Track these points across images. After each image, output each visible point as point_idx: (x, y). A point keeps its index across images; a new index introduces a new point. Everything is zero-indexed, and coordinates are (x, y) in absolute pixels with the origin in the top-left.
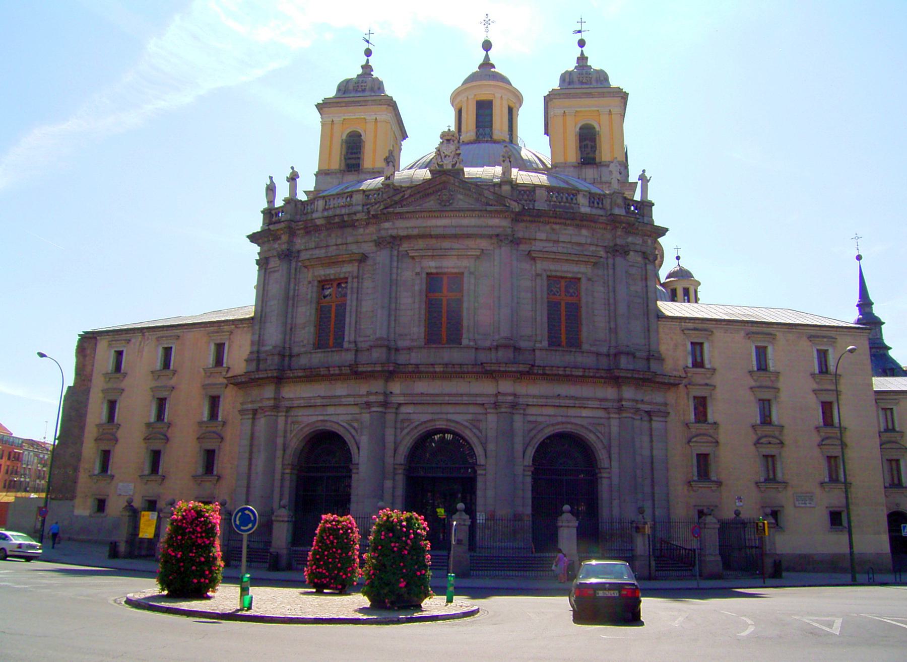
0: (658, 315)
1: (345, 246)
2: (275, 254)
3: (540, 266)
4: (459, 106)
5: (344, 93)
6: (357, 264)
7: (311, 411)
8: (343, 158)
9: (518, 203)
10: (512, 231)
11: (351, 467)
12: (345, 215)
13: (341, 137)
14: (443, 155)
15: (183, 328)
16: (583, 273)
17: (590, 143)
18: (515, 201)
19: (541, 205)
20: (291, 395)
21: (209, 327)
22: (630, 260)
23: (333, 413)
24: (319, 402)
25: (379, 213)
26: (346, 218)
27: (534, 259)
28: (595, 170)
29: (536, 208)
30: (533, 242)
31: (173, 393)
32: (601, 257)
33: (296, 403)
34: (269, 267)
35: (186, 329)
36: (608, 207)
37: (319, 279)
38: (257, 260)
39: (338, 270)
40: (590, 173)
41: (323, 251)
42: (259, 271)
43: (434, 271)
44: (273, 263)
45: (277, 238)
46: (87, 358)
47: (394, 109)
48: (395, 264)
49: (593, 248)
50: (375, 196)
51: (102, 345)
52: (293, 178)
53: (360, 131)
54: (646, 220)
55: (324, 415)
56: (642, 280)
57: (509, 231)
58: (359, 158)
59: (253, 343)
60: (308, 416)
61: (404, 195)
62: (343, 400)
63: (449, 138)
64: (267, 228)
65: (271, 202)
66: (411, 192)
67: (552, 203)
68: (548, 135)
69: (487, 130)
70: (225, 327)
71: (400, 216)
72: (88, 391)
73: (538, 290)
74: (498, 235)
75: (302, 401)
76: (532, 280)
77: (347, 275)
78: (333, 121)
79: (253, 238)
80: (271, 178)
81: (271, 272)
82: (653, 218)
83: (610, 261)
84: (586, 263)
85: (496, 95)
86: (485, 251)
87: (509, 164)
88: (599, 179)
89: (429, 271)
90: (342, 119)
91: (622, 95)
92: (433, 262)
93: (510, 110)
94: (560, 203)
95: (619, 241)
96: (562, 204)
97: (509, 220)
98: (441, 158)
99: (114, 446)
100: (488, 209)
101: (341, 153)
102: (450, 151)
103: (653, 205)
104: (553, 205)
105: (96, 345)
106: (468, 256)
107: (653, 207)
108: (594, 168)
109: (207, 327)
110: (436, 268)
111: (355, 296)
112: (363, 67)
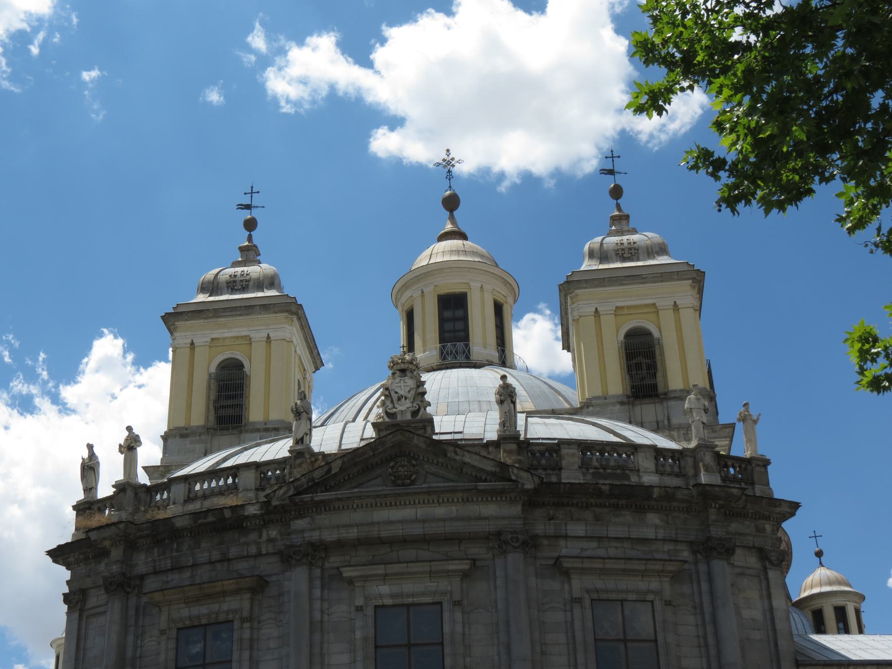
0: (796, 660)
1: (226, 564)
2: (100, 582)
3: (577, 584)
4: (406, 308)
5: (210, 296)
6: (248, 596)
8: (211, 408)
9: (532, 475)
10: (524, 524)
13: (208, 371)
14: (395, 397)
16: (656, 593)
17: (644, 361)
18: (526, 471)
19: (571, 475)
22: (736, 563)
25: (288, 501)
27: (566, 574)
28: (658, 406)
29: (563, 481)
30: (562, 543)
32: (686, 562)
34: (88, 606)
36: (691, 472)
37: (180, 625)
38: (64, 594)
39: (215, 607)
40: (649, 410)
41: (187, 574)
42: (69, 613)
43: (388, 601)
45: (103, 554)
47: (299, 319)
48: (317, 593)
49: (668, 547)
50: (278, 472)
52: (130, 446)
53: (239, 357)
54: (758, 490)
56: (761, 598)
57: (519, 524)
58: (240, 406)
61: (330, 470)
63: (403, 366)
64: (83, 536)
65: (90, 488)
66: (343, 463)
67: (591, 471)
68: (569, 351)
69: (460, 345)
71: (323, 506)
73: (577, 625)
74: (499, 534)
76: (565, 611)
77: (231, 617)
78: (192, 343)
79: (58, 554)
80: (90, 447)
82: (771, 486)
83: (702, 567)
84: (660, 573)
85: (472, 284)
86: (478, 563)
87: (512, 405)
88: (666, 422)
89: (380, 603)
90: (209, 339)
91: (695, 276)
92: (387, 587)
93: (498, 309)
94: (605, 469)
95: (716, 532)
96: (609, 471)
97: (519, 507)
98: (392, 402)
100: (480, 488)
101: (208, 397)
102: (408, 389)
103: (766, 463)
104: (593, 473)
106: (448, 574)
107: (769, 468)
108: (655, 403)
110: (392, 596)
111: (246, 654)
112: (242, 249)
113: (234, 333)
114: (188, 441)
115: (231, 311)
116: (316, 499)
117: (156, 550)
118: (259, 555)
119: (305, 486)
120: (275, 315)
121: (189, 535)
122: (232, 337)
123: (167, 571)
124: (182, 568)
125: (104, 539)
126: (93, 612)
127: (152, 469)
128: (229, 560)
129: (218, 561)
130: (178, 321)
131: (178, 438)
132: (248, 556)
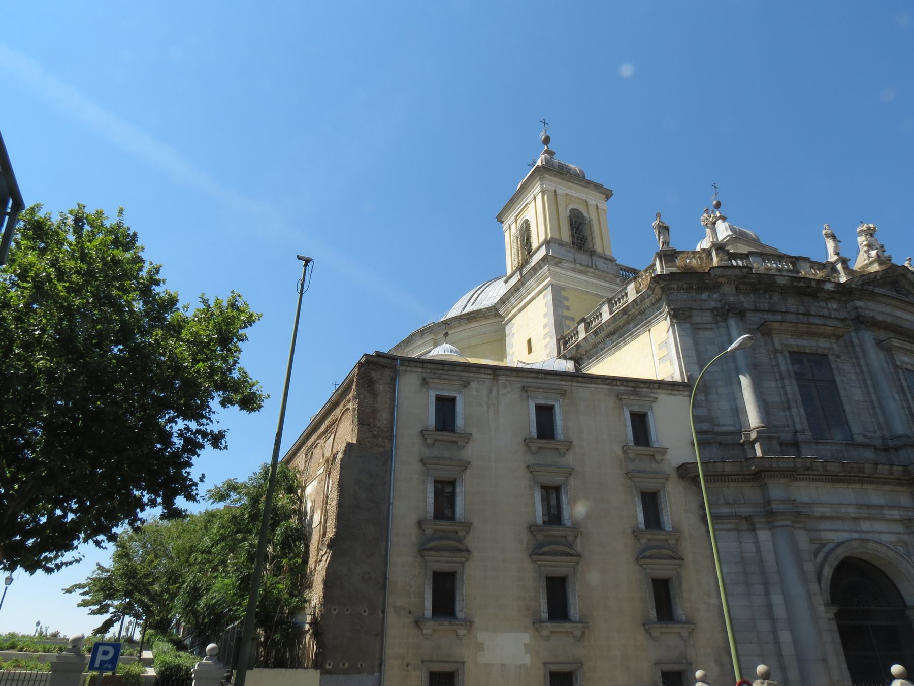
1: (806, 317)
7: (837, 525)
12: (814, 279)
15: (575, 379)
20: (806, 499)
21: (619, 386)
24: (852, 511)
33: (818, 511)
37: (790, 349)
39: (814, 343)
41: (779, 317)
46: (380, 399)
51: (408, 384)
55: (859, 532)
59: (697, 419)
60: (836, 531)
62: (886, 512)
63: (872, 232)
70: (645, 390)
72: (387, 457)
77: (826, 352)
90: (565, 193)
99: (463, 563)
105: (393, 380)
109: (616, 385)
113: (578, 195)
115: (578, 181)
116: (876, 291)
117: (752, 295)
118: (830, 317)
119: (866, 281)
120: (598, 194)
121: (780, 291)
122: (576, 197)
123: (763, 311)
125: (724, 276)
126: (699, 326)
127: (551, 257)
128: (810, 315)
129: (802, 314)
132: (823, 316)
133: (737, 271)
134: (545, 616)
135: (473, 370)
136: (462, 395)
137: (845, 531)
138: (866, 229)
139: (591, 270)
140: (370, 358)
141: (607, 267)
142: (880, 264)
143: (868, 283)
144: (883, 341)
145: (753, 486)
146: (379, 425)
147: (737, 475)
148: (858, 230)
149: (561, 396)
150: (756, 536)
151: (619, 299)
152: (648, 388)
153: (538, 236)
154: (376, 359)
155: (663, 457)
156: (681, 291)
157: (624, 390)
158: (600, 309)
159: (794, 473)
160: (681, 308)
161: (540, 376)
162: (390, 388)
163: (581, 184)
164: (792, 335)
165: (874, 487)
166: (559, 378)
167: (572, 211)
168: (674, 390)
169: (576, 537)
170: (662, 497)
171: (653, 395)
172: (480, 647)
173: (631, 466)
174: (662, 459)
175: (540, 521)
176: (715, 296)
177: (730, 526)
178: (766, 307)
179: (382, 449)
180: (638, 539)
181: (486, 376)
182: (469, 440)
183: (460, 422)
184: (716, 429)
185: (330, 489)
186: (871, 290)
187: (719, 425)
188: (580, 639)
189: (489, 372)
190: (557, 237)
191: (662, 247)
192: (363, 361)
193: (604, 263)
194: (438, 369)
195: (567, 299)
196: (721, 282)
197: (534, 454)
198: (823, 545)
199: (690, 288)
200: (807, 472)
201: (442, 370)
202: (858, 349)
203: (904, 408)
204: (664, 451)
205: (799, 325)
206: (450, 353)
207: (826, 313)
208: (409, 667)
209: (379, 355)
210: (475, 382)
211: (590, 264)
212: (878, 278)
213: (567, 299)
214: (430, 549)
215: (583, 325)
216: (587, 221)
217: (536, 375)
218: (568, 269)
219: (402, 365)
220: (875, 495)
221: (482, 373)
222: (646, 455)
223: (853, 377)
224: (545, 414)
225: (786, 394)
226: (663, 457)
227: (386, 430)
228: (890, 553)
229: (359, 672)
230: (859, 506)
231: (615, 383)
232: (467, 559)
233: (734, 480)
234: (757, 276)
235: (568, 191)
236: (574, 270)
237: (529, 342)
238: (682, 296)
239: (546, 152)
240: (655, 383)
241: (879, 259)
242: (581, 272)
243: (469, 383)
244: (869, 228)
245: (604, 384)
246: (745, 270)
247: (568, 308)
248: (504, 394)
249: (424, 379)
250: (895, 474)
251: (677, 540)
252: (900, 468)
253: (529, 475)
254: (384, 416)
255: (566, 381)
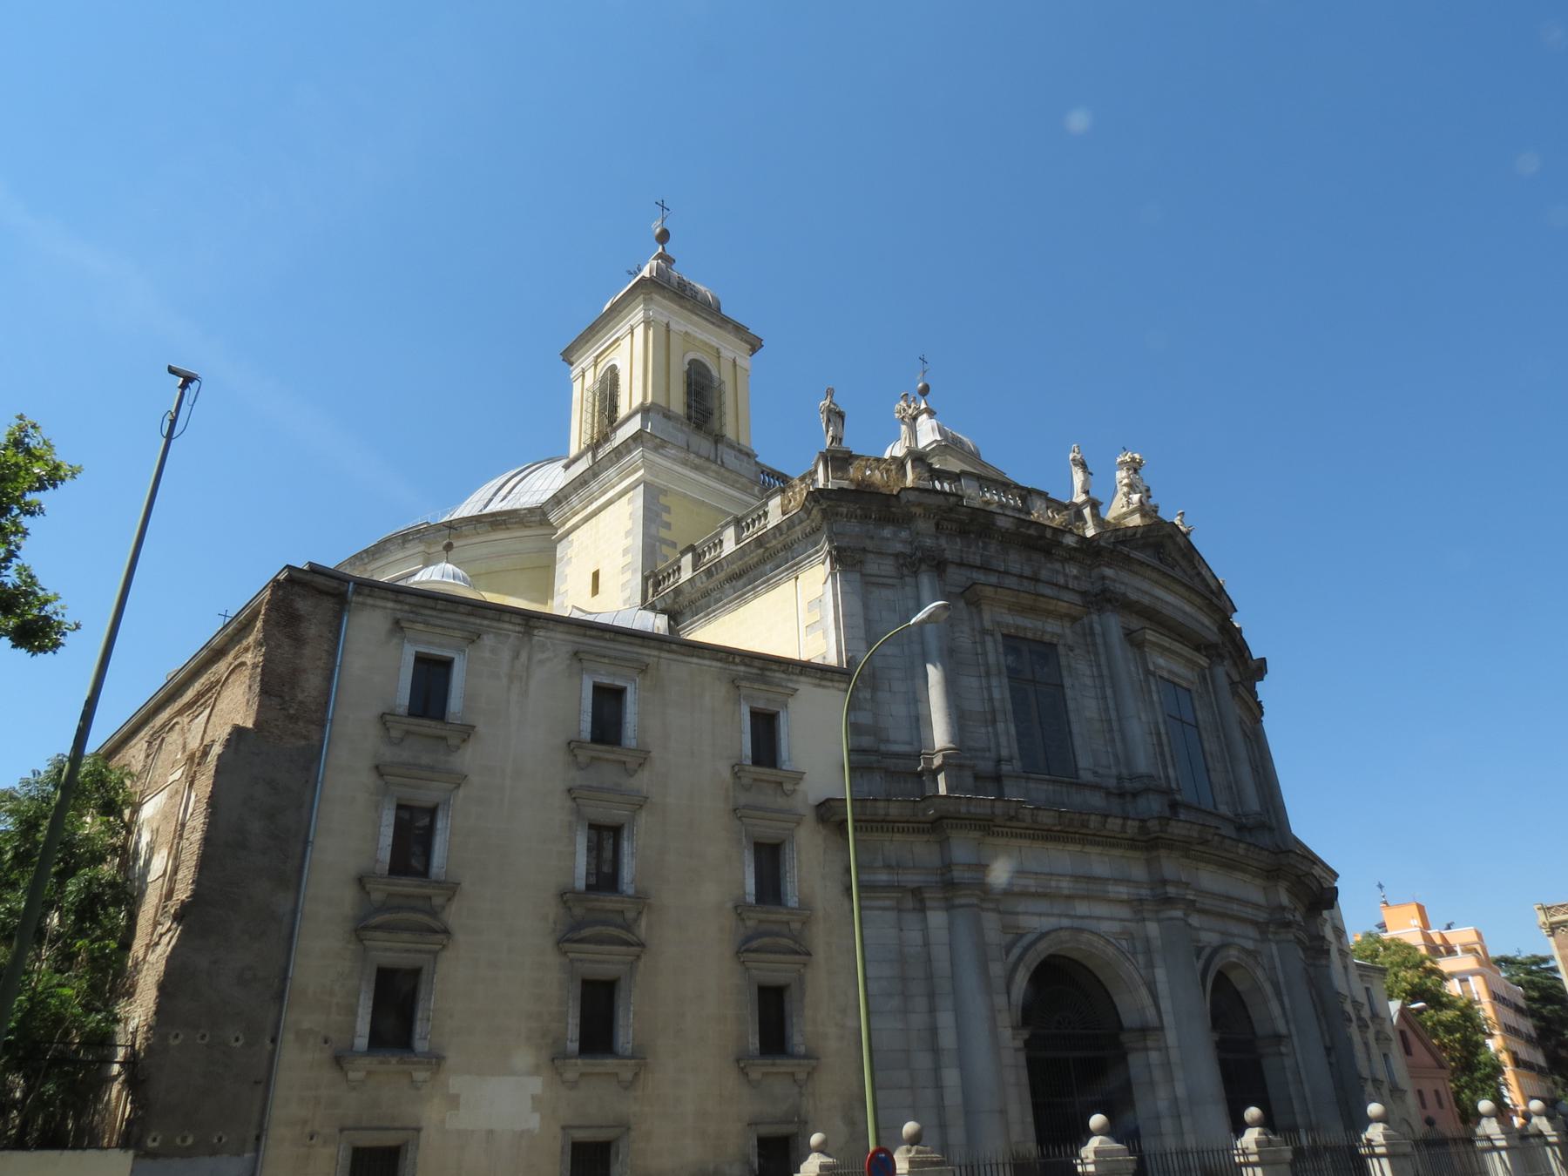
1: (1033, 583)
7: (1043, 905)
11: (1124, 1037)
12: (1049, 527)
21: (737, 664)
23: (1088, 914)
24: (1066, 886)
25: (1111, 547)
26: (1049, 534)
31: (643, 819)
35: (670, 651)
39: (1039, 624)
41: (993, 579)
44: (876, 566)
46: (307, 651)
59: (854, 729)
60: (1040, 915)
61: (1135, 534)
62: (1110, 888)
63: (1136, 466)
70: (777, 675)
72: (309, 760)
75: (1032, 882)
77: (1055, 640)
81: (873, 584)
99: (435, 954)
105: (338, 617)
109: (733, 663)
113: (704, 337)
114: (671, 423)
116: (1132, 555)
117: (958, 540)
118: (1067, 588)
119: (1121, 539)
121: (1000, 538)
122: (701, 341)
123: (972, 567)
124: (991, 570)
125: (920, 505)
126: (874, 579)
127: (649, 436)
129: (1027, 578)
130: (656, 294)
131: (661, 415)
132: (1056, 585)
133: (940, 500)
134: (574, 1046)
135: (490, 614)
136: (464, 655)
137: (1052, 915)
138: (1129, 460)
139: (714, 467)
140: (295, 574)
141: (741, 465)
142: (1143, 516)
143: (1123, 543)
144: (1135, 631)
145: (928, 841)
146: (300, 697)
147: (907, 822)
148: (1119, 460)
149: (640, 673)
150: (925, 919)
151: (754, 521)
152: (783, 672)
153: (631, 396)
154: (308, 577)
155: (797, 787)
156: (853, 520)
157: (744, 672)
158: (720, 533)
159: (991, 823)
160: (849, 548)
161: (607, 636)
162: (330, 632)
163: (712, 320)
164: (1009, 609)
165: (1098, 850)
166: (639, 641)
167: (693, 362)
168: (826, 679)
169: (640, 913)
170: (787, 851)
171: (790, 685)
172: (454, 1101)
173: (743, 799)
174: (794, 790)
175: (581, 884)
176: (904, 534)
177: (888, 903)
178: (978, 561)
179: (303, 743)
180: (743, 920)
181: (511, 627)
182: (469, 736)
183: (455, 704)
184: (883, 747)
185: (190, 810)
186: (1126, 553)
187: (888, 741)
188: (628, 1086)
189: (518, 620)
190: (663, 404)
191: (831, 444)
192: (281, 577)
193: (735, 457)
194: (424, 607)
195: (667, 510)
196: (915, 514)
197: (583, 769)
198: (1021, 936)
199: (866, 517)
200: (1008, 823)
201: (432, 608)
202: (1099, 640)
203: (1151, 734)
204: (798, 777)
205: (1022, 594)
206: (452, 581)
207: (1061, 581)
208: (315, 1139)
209: (315, 569)
210: (491, 636)
211: (712, 457)
212: (1138, 536)
213: (667, 510)
214: (377, 928)
215: (689, 556)
216: (716, 384)
217: (600, 634)
218: (674, 460)
219: (357, 592)
220: (1099, 863)
221: (504, 621)
222: (768, 781)
223: (1088, 681)
224: (608, 700)
225: (991, 699)
226: (797, 787)
227: (313, 708)
228: (1110, 950)
229: (214, 1152)
230: (1076, 878)
231: (731, 659)
232: (444, 946)
233: (901, 830)
234: (969, 510)
235: (689, 331)
236: (684, 463)
237: (596, 576)
238: (854, 527)
239: (660, 256)
240: (796, 665)
241: (1142, 509)
242: (696, 468)
243: (479, 637)
244: (1133, 460)
245: (714, 659)
246: (952, 499)
247: (668, 526)
248: (541, 662)
249: (397, 622)
250: (1129, 831)
251: (804, 923)
252: (1136, 823)
253: (569, 803)
254: (312, 682)
255: (649, 647)
